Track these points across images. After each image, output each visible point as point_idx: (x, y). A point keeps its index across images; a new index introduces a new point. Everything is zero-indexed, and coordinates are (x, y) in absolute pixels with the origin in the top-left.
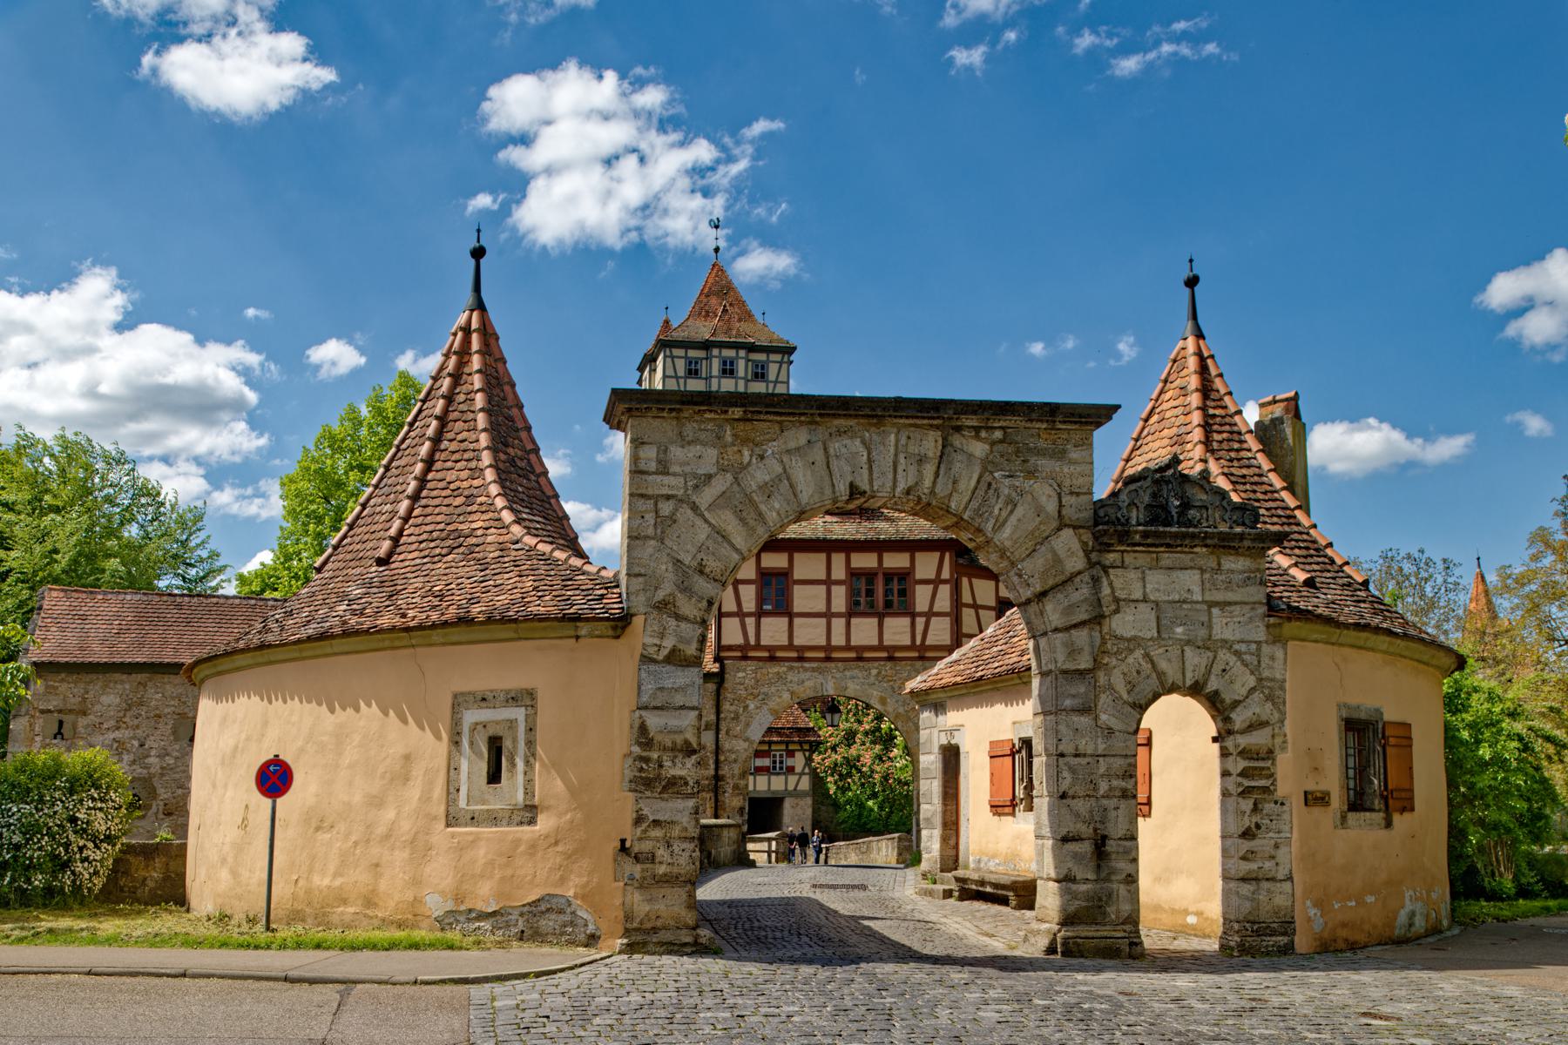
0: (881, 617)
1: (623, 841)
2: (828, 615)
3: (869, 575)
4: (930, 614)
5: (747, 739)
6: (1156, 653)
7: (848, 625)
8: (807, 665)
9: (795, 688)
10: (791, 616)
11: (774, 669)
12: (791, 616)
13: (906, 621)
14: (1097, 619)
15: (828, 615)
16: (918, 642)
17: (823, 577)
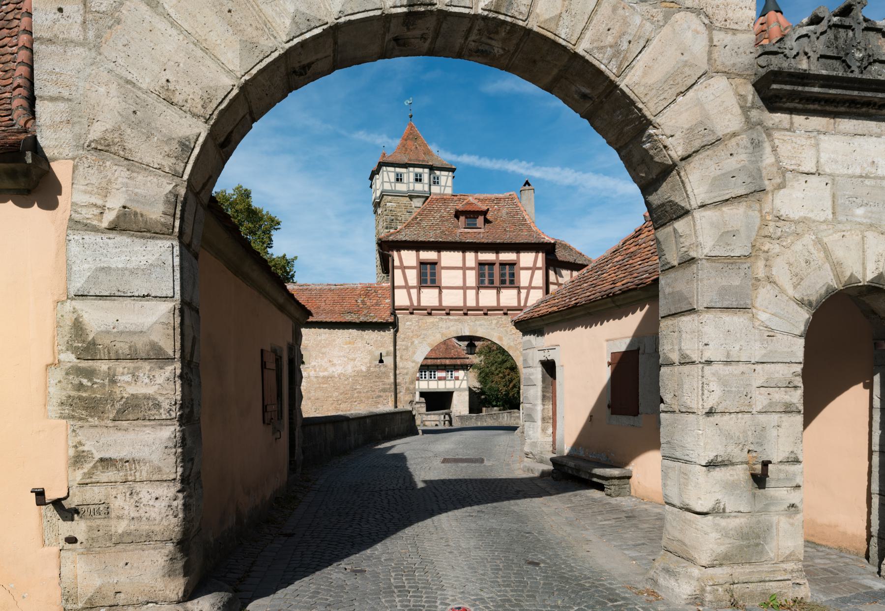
0: (498, 289)
1: (40, 494)
2: (464, 288)
3: (491, 264)
4: (529, 288)
5: (414, 362)
6: (831, 239)
7: (477, 294)
8: (450, 317)
9: (444, 331)
10: (440, 288)
11: (430, 319)
12: (440, 288)
13: (515, 291)
14: (757, 193)
15: (464, 288)
16: (522, 304)
17: (461, 265)
